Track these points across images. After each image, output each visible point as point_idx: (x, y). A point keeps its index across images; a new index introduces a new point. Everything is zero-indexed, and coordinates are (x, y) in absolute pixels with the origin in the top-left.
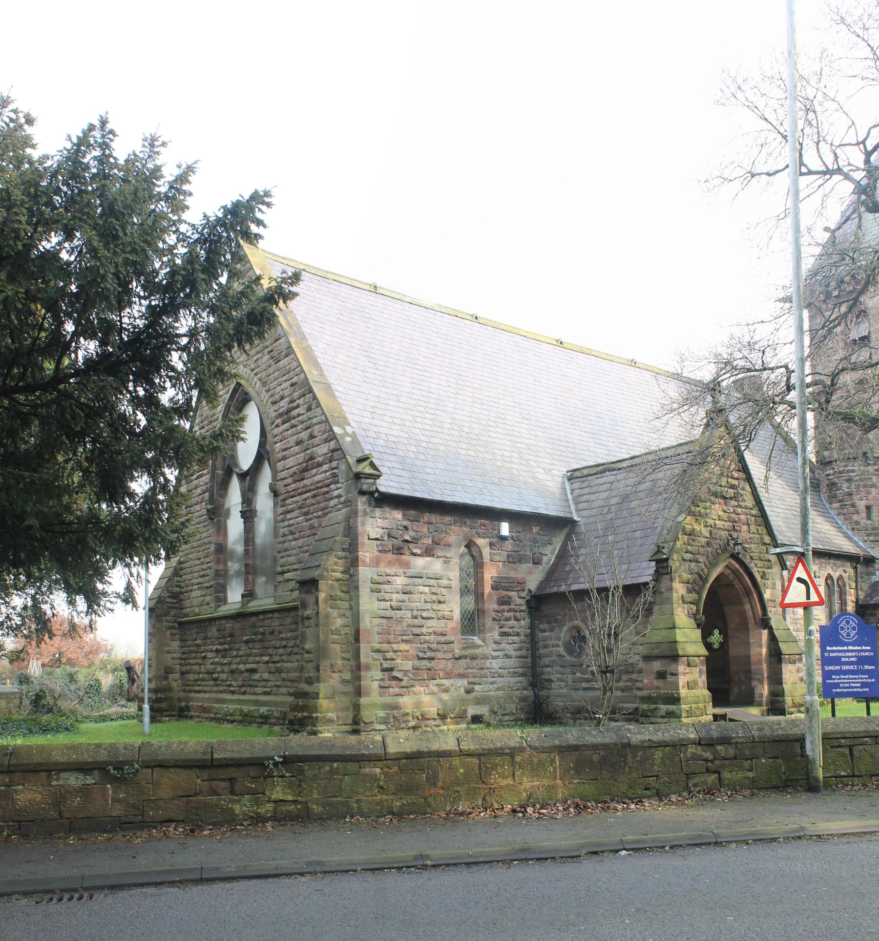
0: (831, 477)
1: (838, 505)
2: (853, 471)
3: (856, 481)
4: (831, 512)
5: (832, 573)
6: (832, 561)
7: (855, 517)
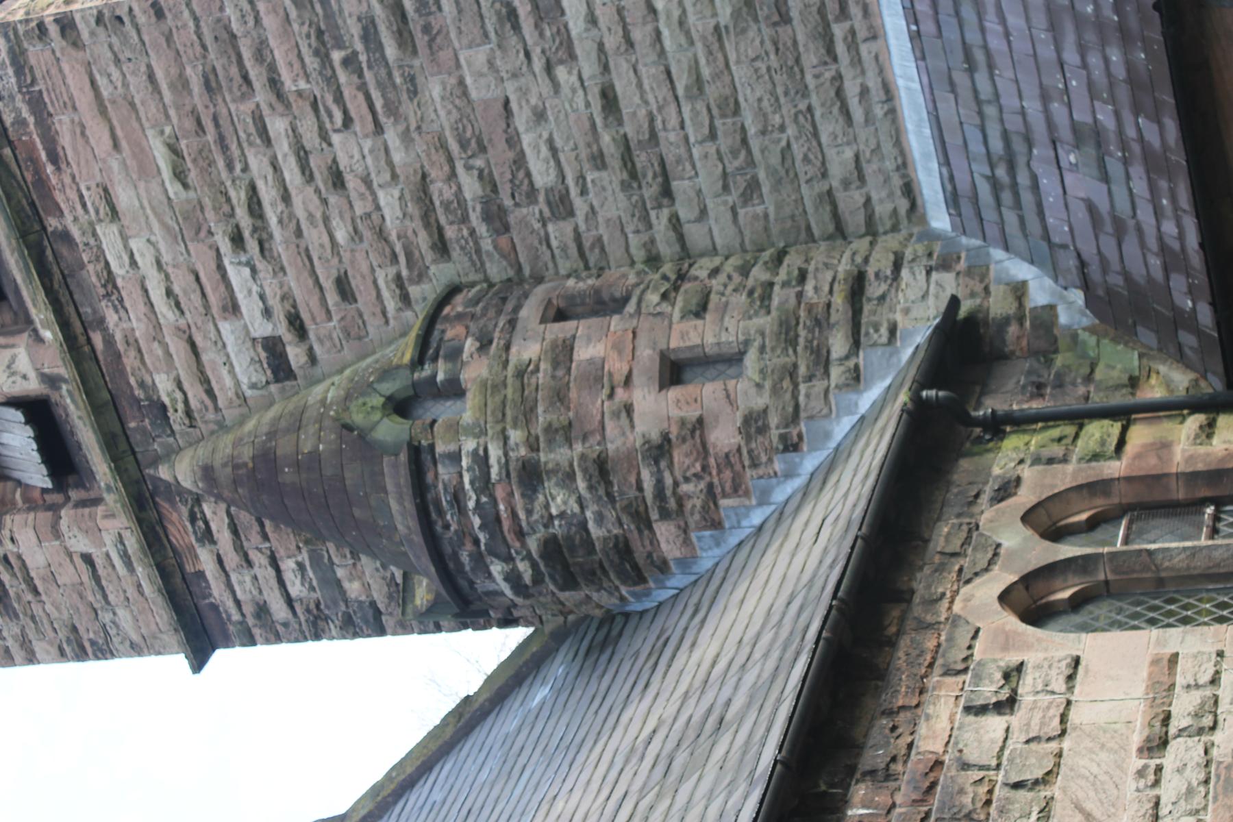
0: (523, 567)
1: (665, 532)
2: (482, 460)
3: (533, 446)
4: (706, 563)
5: (1001, 578)
6: (920, 585)
7: (724, 437)
